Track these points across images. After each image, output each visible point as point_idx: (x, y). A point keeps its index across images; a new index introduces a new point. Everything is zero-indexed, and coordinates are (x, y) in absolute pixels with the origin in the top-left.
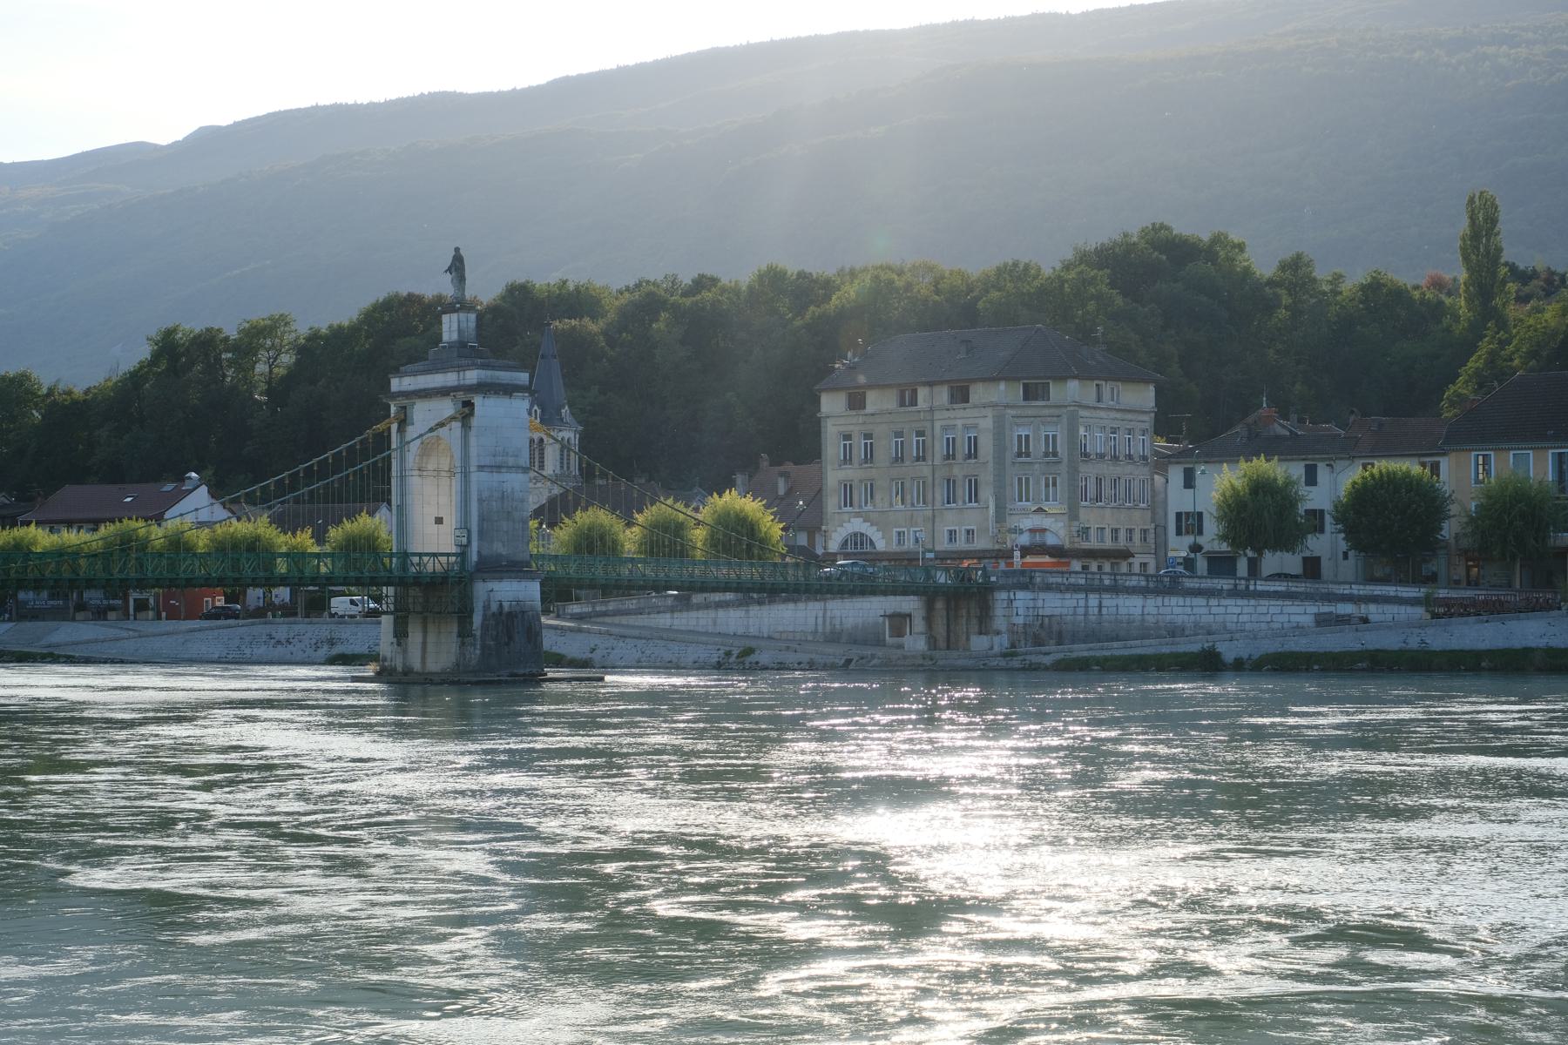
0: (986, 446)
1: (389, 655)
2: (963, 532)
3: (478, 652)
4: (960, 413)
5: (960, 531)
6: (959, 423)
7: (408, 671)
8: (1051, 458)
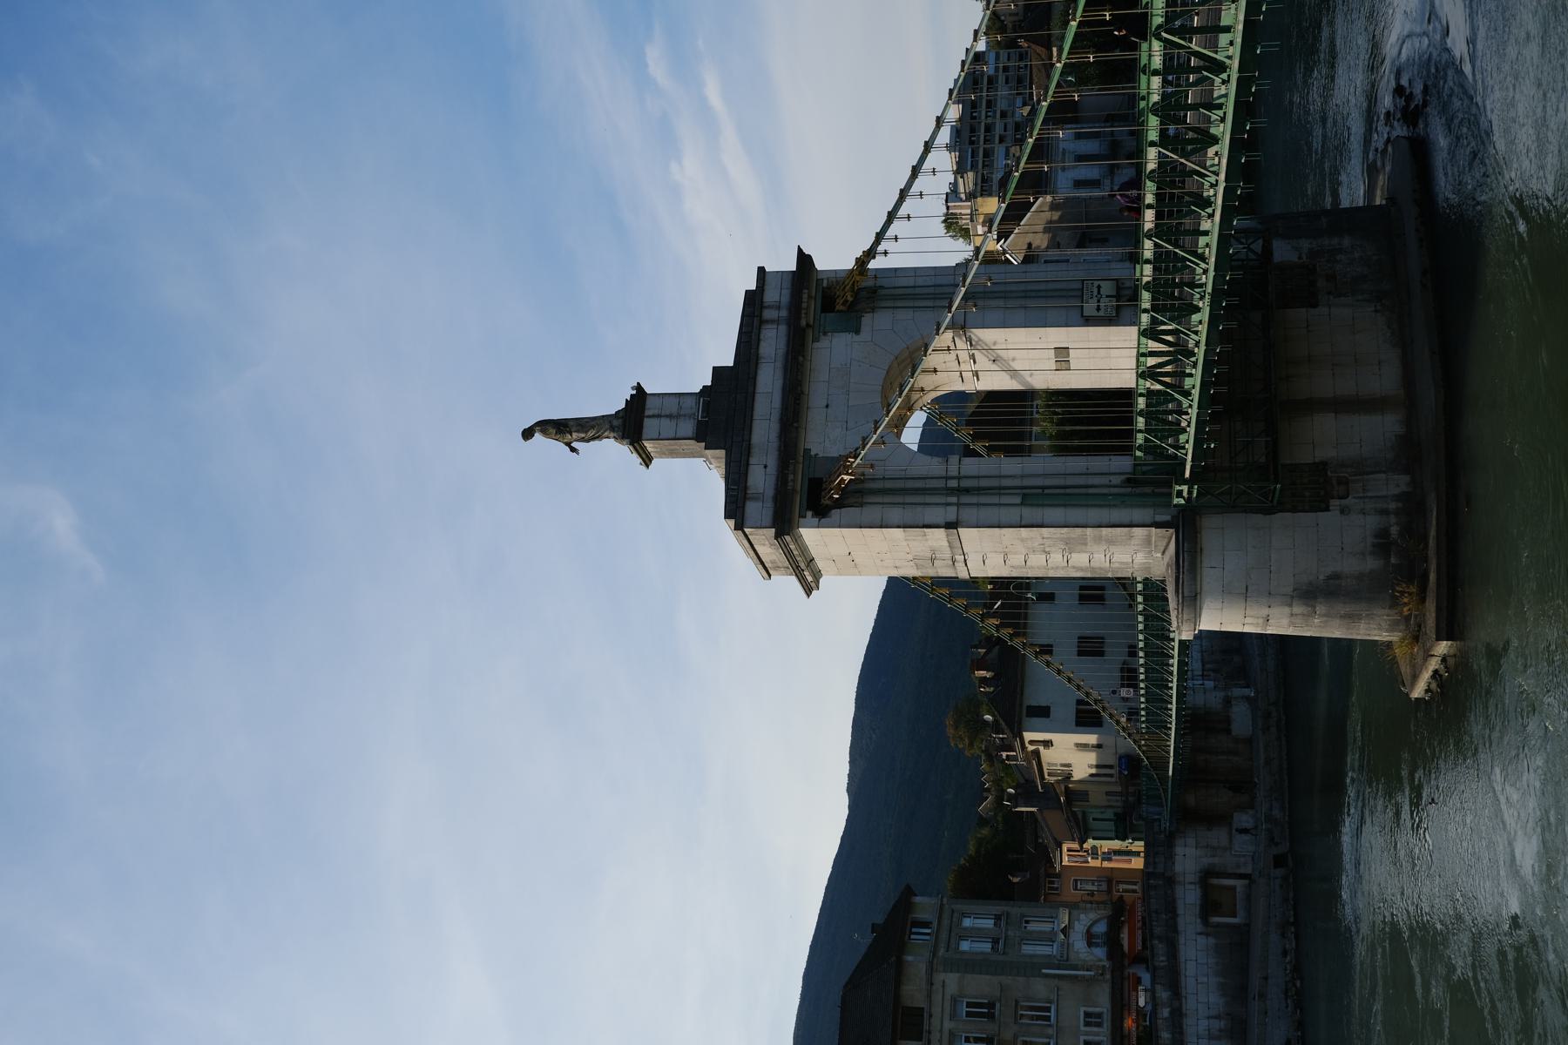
0: (981, 986)
1: (1372, 522)
2: (1088, 1029)
3: (1346, 242)
4: (936, 1022)
5: (1087, 1034)
6: (948, 1025)
7: (1407, 454)
8: (1003, 923)
